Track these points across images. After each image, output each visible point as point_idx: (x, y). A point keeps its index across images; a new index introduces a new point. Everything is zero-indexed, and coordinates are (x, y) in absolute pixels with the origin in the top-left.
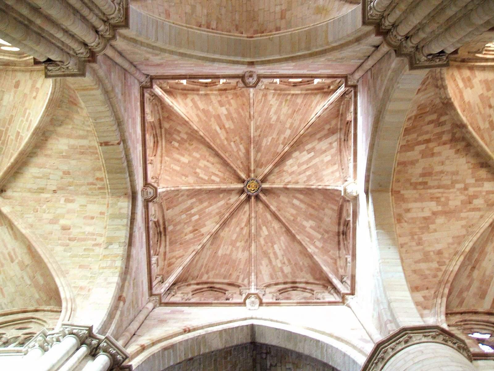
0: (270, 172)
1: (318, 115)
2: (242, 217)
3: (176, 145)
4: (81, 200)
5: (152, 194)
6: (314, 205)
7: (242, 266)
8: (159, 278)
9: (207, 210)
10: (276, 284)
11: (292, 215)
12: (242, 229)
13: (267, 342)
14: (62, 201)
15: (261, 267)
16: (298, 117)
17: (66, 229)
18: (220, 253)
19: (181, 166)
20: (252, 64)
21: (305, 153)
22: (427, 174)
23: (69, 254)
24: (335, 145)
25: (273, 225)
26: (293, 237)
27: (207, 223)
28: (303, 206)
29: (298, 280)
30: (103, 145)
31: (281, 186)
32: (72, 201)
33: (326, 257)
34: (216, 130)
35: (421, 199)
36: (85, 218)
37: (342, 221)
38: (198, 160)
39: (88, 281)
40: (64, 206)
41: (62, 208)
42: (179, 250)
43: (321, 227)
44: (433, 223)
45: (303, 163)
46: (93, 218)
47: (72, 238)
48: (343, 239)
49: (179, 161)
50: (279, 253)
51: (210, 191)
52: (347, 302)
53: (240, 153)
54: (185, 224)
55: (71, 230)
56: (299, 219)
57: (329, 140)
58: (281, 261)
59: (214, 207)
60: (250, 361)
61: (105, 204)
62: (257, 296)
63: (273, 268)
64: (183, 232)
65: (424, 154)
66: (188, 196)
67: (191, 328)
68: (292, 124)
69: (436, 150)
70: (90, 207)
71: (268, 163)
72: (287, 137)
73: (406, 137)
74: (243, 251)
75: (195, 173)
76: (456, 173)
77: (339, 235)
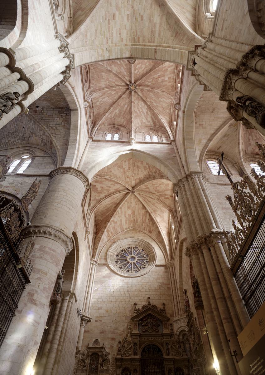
0: (138, 95)
4: (128, 27)
7: (98, 85)
9: (122, 67)
11: (121, 104)
12: (114, 83)
13: (72, 116)
14: (128, 13)
18: (103, 74)
22: (138, 167)
26: (112, 105)
27: (116, 68)
28: (125, 109)
29: (94, 109)
31: (133, 100)
32: (128, 20)
36: (120, 29)
38: (145, 65)
39: (90, 39)
44: (121, 169)
45: (142, 109)
46: (120, 34)
50: (105, 100)
51: (131, 69)
56: (119, 107)
59: (124, 70)
63: (98, 98)
69: (146, 170)
71: (143, 94)
75: (139, 63)
76: (138, 174)
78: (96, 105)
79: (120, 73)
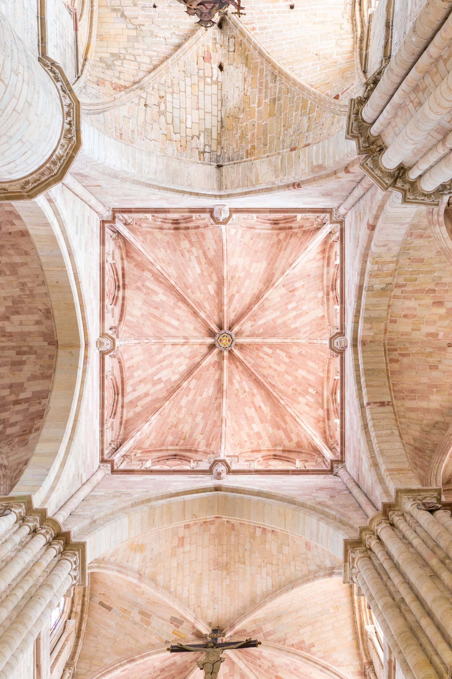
0: (205, 356)
1: (148, 423)
2: (237, 306)
3: (311, 390)
5: (335, 341)
6: (154, 320)
8: (334, 237)
9: (278, 313)
10: (197, 227)
11: (180, 308)
12: (238, 292)
15: (215, 248)
16: (172, 420)
17: (438, 302)
18: (263, 265)
19: (306, 365)
20: (217, 489)
21: (164, 379)
23: (436, 274)
24: (128, 389)
25: (202, 296)
27: (278, 299)
28: (167, 318)
29: (172, 231)
30: (386, 403)
33: (139, 259)
34: (266, 406)
35: (23, 335)
36: (415, 316)
37: (120, 302)
38: (286, 372)
40: (440, 329)
41: (442, 327)
42: (312, 268)
43: (145, 294)
44: (7, 307)
46: (405, 316)
47: (431, 293)
48: (118, 281)
49: (309, 372)
52: (111, 213)
53: (239, 378)
54: (304, 299)
55: (432, 301)
56: (171, 304)
57: (136, 394)
58: (193, 254)
60: (225, 143)
61: (390, 332)
62: (217, 221)
63: (201, 246)
64: (307, 289)
65: (21, 387)
66: (299, 332)
67: (292, 188)
68: (179, 412)
70: (408, 329)
71: (207, 368)
72: (185, 397)
73: (41, 409)
74: (236, 267)
75: (290, 357)
77: (124, 285)
78: (182, 237)
79: (263, 309)
